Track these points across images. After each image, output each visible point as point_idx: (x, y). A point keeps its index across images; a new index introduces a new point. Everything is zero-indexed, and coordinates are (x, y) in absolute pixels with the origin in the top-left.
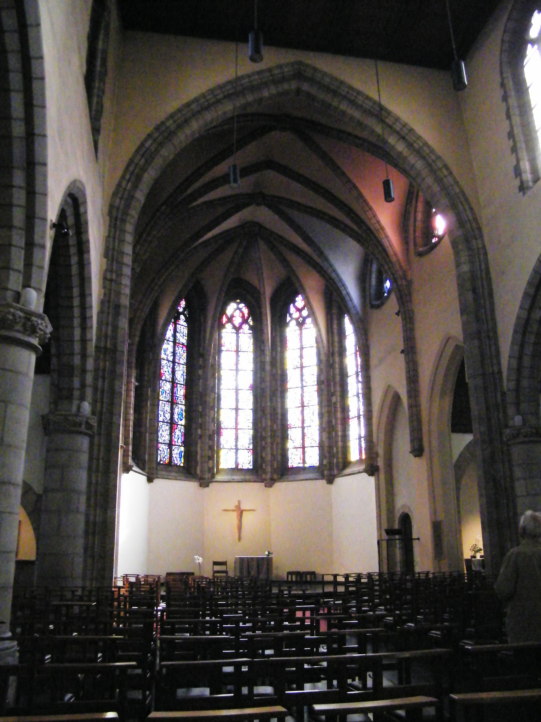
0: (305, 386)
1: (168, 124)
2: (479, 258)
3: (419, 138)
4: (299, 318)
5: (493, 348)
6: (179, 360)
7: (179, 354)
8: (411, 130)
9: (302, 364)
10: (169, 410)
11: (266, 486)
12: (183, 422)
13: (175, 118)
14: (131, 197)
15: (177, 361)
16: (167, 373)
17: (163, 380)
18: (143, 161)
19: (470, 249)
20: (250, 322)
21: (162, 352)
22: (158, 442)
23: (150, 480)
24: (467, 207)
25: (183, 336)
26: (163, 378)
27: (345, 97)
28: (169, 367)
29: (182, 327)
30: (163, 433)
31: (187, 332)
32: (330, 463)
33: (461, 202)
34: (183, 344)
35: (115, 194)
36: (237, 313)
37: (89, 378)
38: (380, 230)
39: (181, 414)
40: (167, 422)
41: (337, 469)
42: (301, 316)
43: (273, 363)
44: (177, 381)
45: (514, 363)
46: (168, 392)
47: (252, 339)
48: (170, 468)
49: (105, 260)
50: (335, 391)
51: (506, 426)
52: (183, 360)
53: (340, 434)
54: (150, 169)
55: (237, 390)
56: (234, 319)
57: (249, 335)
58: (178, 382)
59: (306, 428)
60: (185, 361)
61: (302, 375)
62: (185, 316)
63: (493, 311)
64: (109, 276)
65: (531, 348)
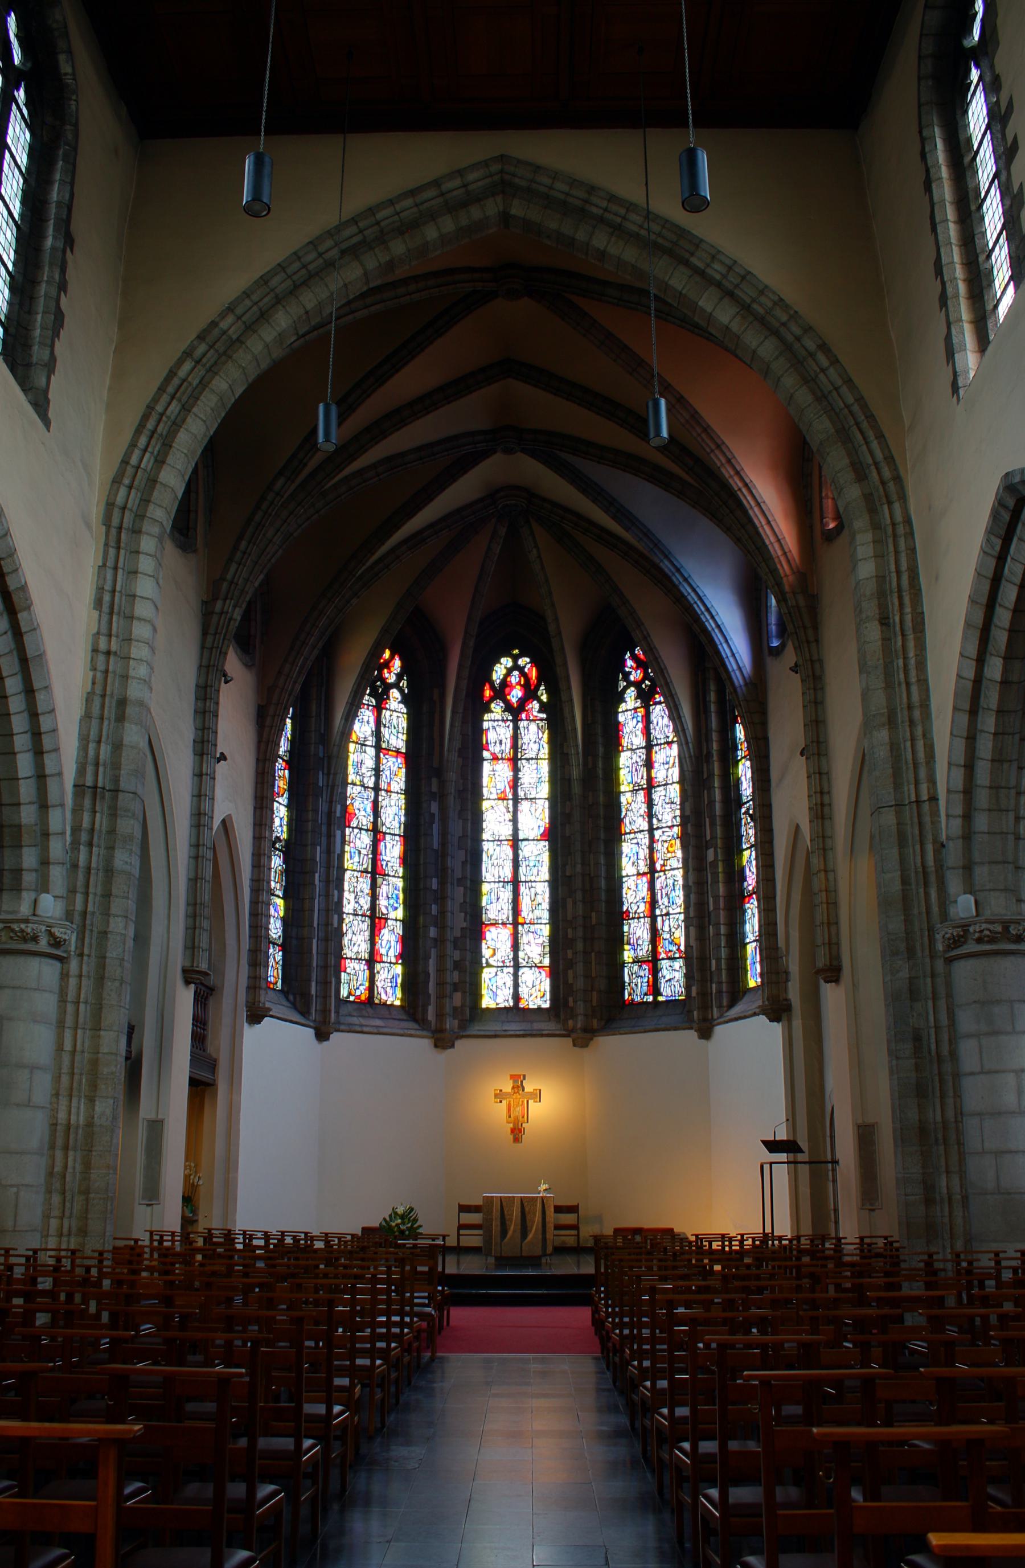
0: (658, 828)
1: (224, 325)
2: (896, 546)
3: (764, 290)
4: (643, 681)
5: (920, 744)
6: (389, 784)
7: (388, 773)
8: (746, 276)
9: (650, 780)
10: (367, 890)
11: (574, 1045)
12: (400, 914)
13: (239, 311)
14: (153, 481)
15: (383, 785)
16: (363, 813)
17: (353, 828)
18: (175, 407)
19: (876, 526)
20: (542, 694)
21: (351, 770)
22: (340, 957)
23: (322, 1036)
24: (871, 434)
25: (398, 732)
26: (354, 823)
27: (601, 220)
28: (367, 799)
29: (395, 714)
30: (354, 938)
31: (405, 725)
32: (704, 994)
33: (857, 424)
34: (398, 752)
35: (117, 481)
36: (515, 678)
37: (57, 848)
38: (744, 490)
39: (394, 896)
40: (362, 915)
41: (720, 1006)
42: (646, 676)
43: (589, 779)
44: (384, 829)
45: (959, 775)
46: (364, 852)
47: (547, 731)
48: (370, 1010)
49: (96, 614)
50: (714, 837)
51: (944, 916)
52: (399, 783)
53: (723, 930)
54: (189, 420)
55: (515, 842)
56: (507, 690)
57: (541, 724)
58: (388, 831)
59: (659, 919)
60: (403, 785)
61: (650, 803)
62: (401, 690)
63: (921, 665)
64: (103, 646)
65: (990, 745)
